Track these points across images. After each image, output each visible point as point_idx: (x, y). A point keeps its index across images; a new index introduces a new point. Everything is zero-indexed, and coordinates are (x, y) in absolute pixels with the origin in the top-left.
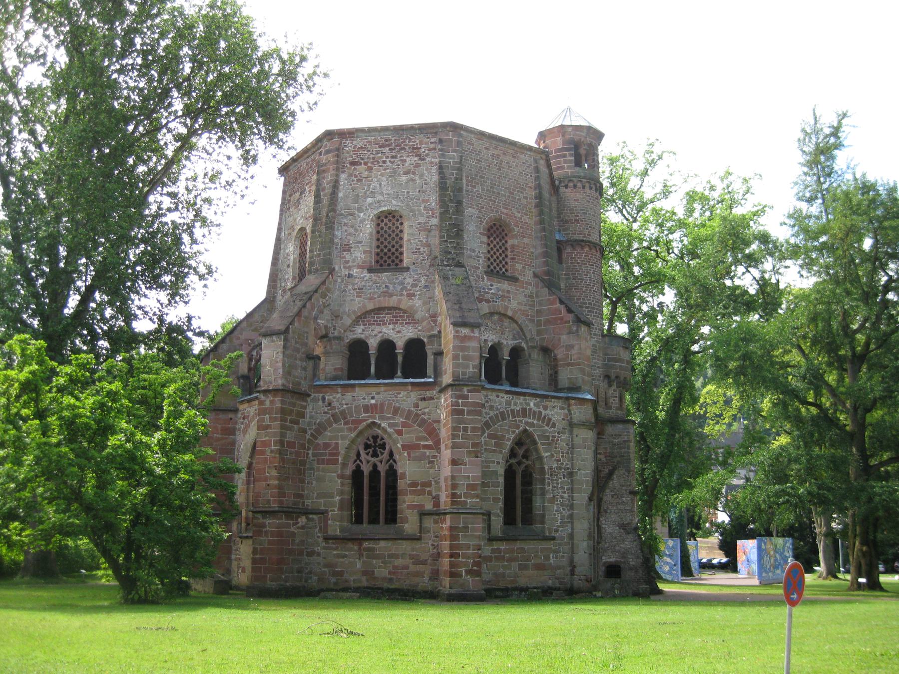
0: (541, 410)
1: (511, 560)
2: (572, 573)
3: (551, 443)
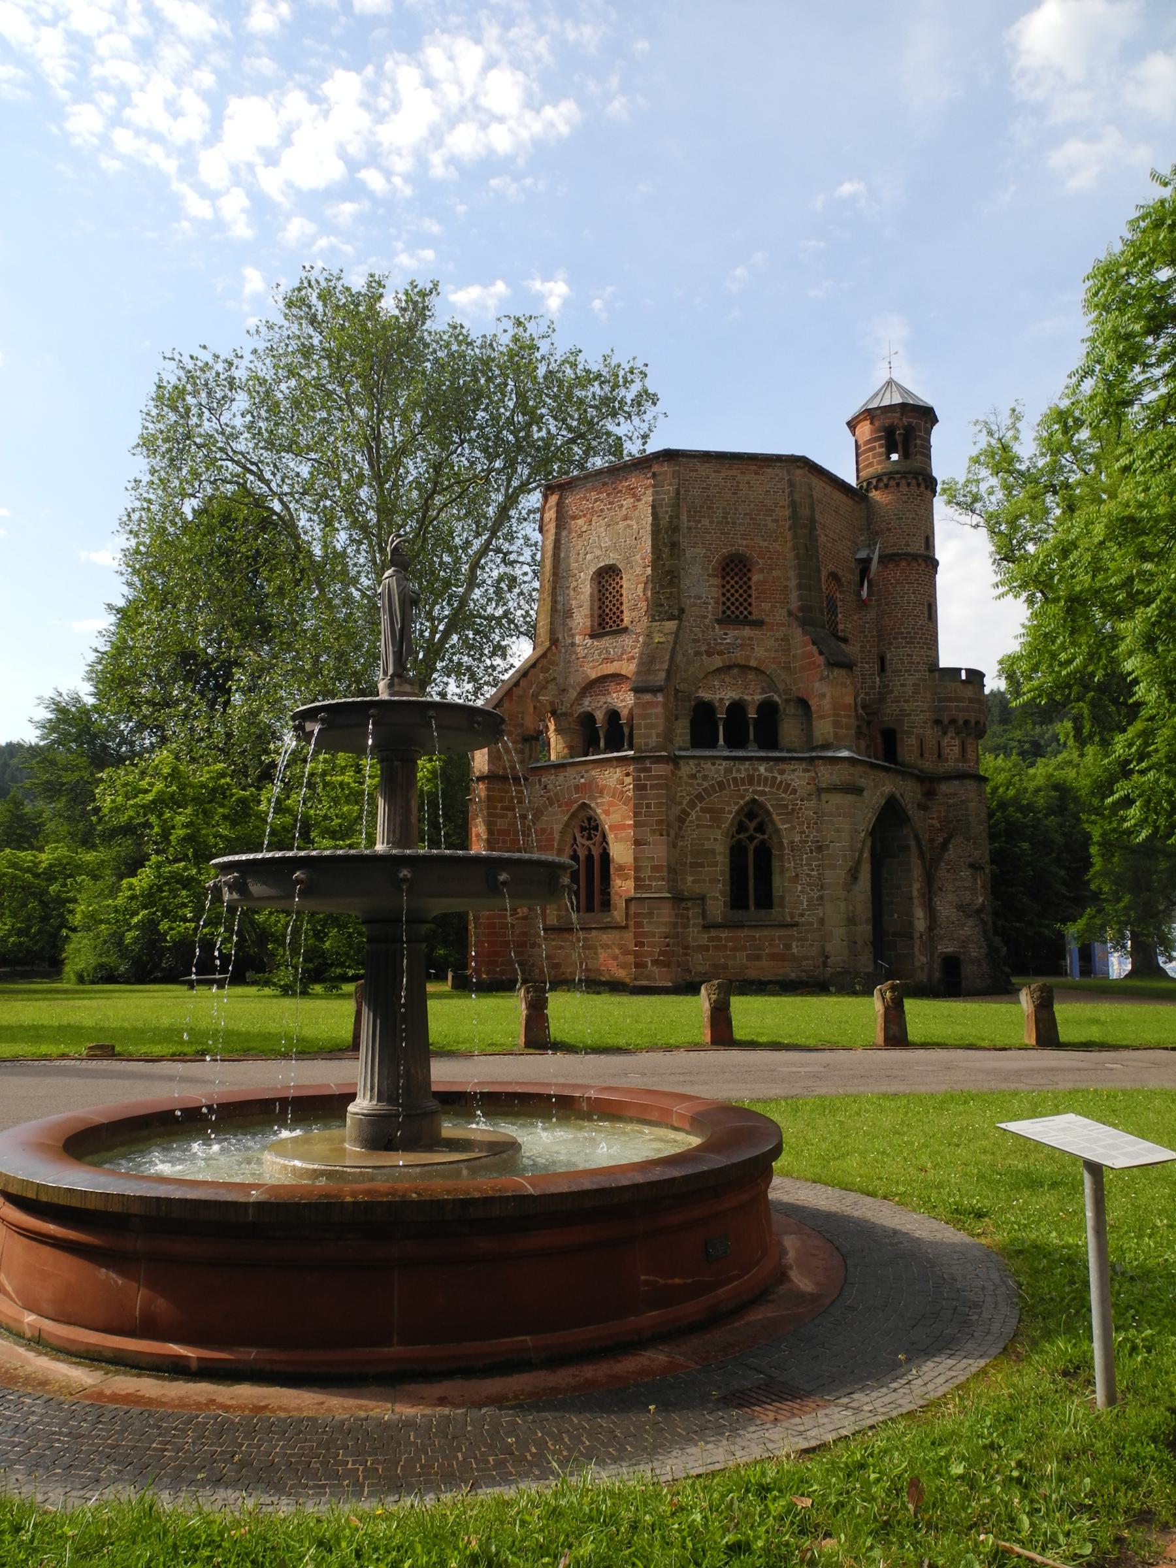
0: (776, 774)
1: (734, 949)
2: (825, 965)
3: (790, 813)
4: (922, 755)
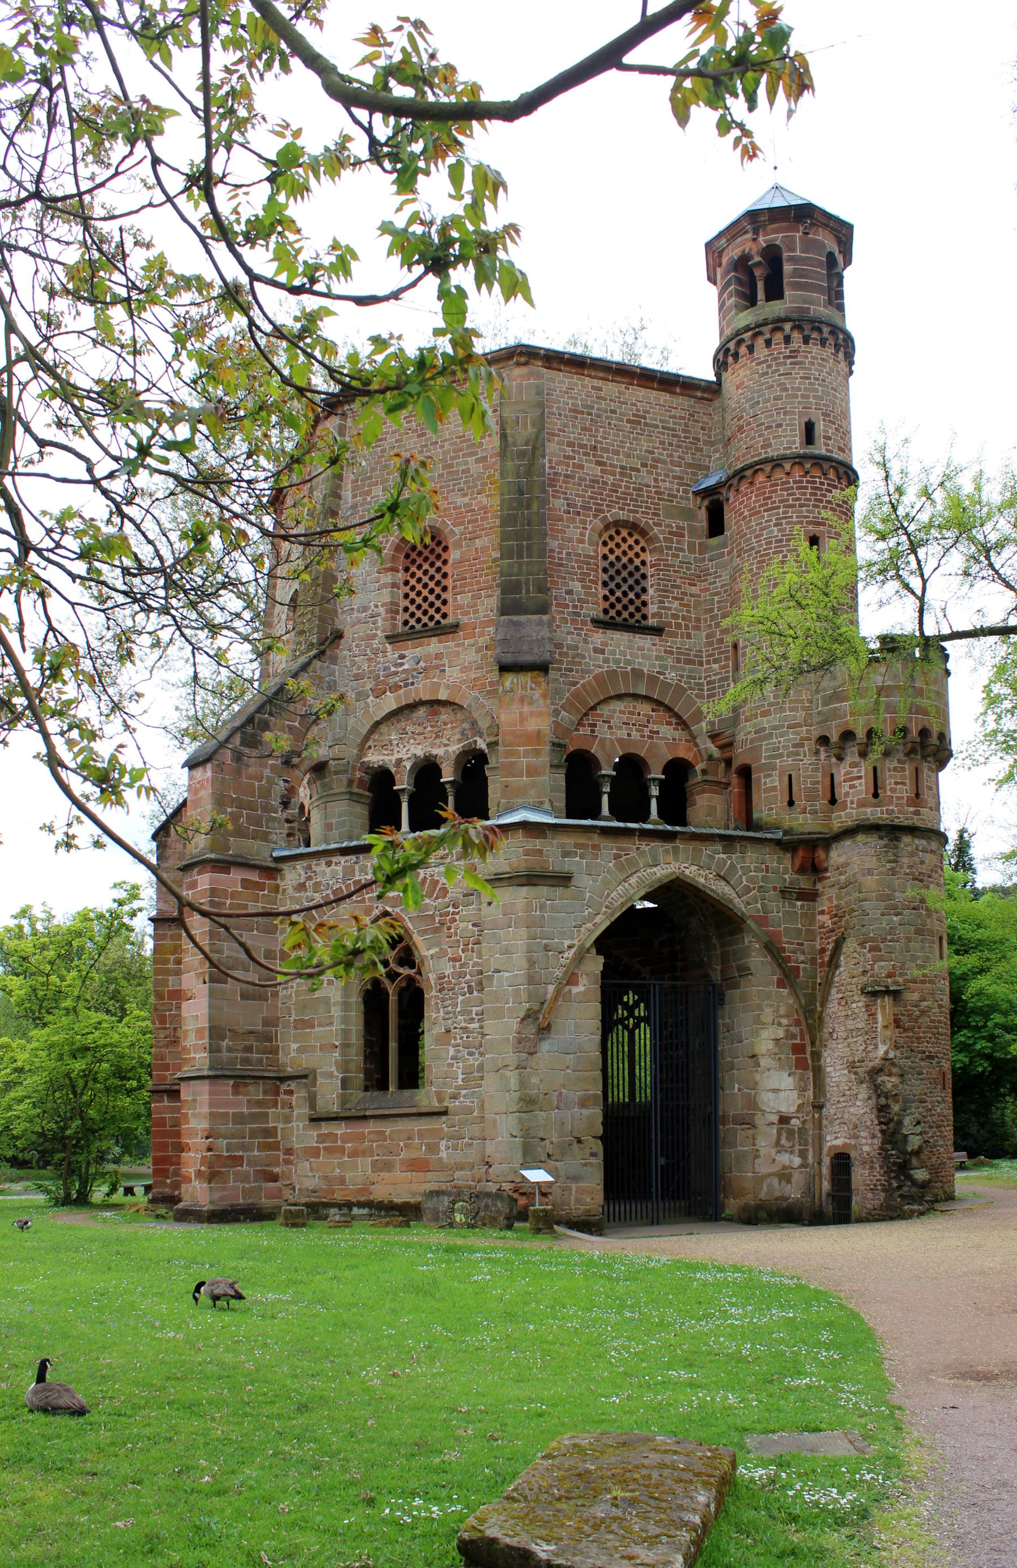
4: (791, 803)
